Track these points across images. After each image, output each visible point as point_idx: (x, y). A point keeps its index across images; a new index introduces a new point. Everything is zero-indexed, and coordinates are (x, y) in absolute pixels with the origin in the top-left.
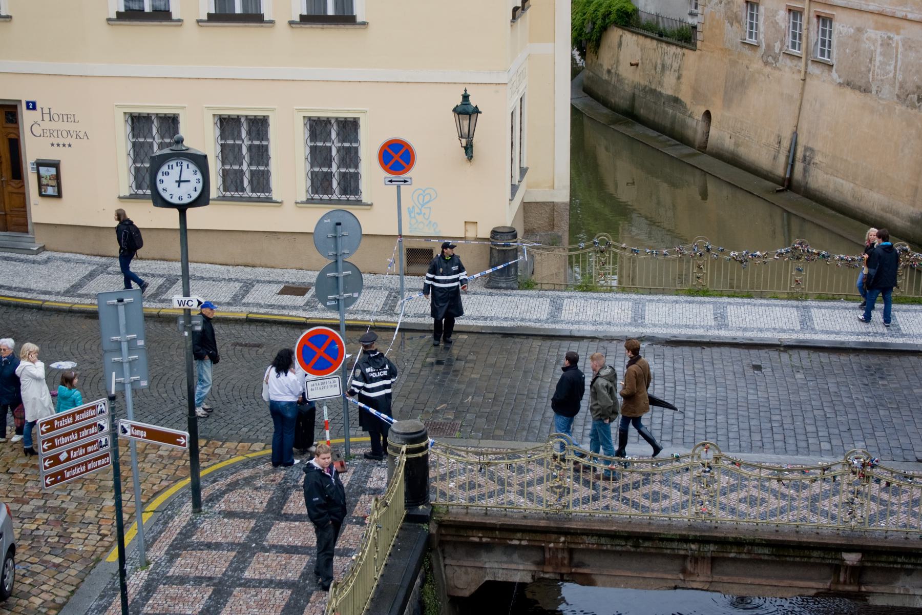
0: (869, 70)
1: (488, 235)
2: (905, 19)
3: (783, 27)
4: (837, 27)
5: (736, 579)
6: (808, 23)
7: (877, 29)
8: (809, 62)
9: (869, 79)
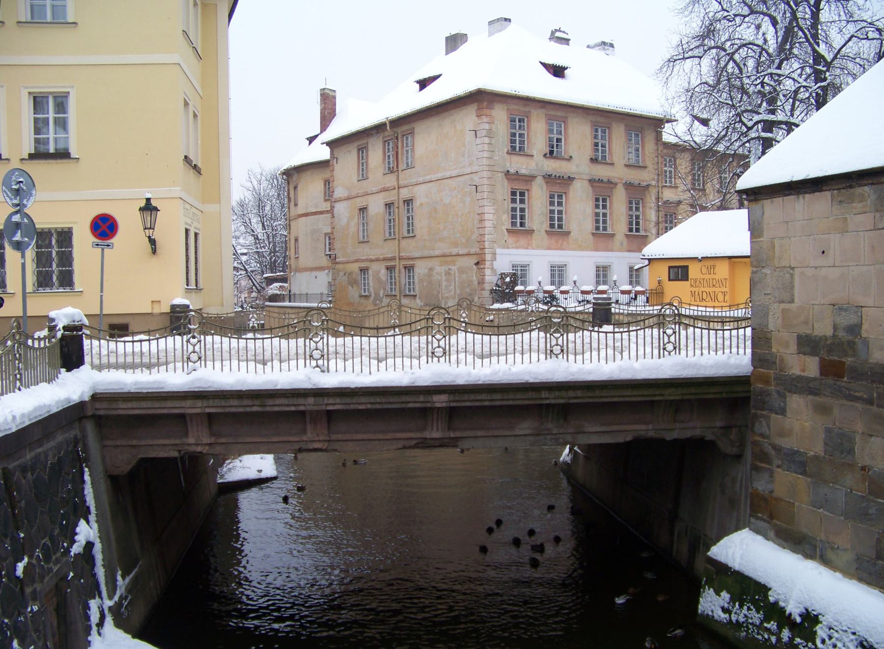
0: (439, 293)
1: (168, 310)
2: (458, 255)
3: (384, 280)
4: (417, 270)
5: (348, 436)
6: (400, 272)
7: (441, 265)
8: (402, 297)
9: (439, 297)
